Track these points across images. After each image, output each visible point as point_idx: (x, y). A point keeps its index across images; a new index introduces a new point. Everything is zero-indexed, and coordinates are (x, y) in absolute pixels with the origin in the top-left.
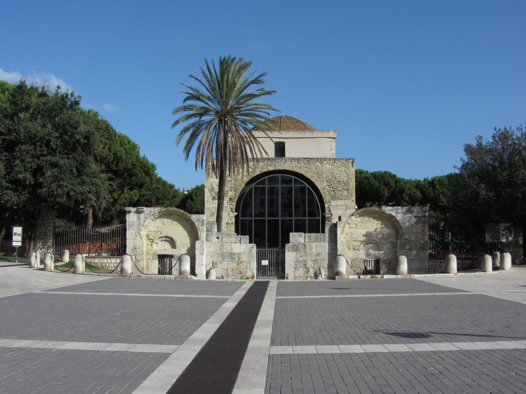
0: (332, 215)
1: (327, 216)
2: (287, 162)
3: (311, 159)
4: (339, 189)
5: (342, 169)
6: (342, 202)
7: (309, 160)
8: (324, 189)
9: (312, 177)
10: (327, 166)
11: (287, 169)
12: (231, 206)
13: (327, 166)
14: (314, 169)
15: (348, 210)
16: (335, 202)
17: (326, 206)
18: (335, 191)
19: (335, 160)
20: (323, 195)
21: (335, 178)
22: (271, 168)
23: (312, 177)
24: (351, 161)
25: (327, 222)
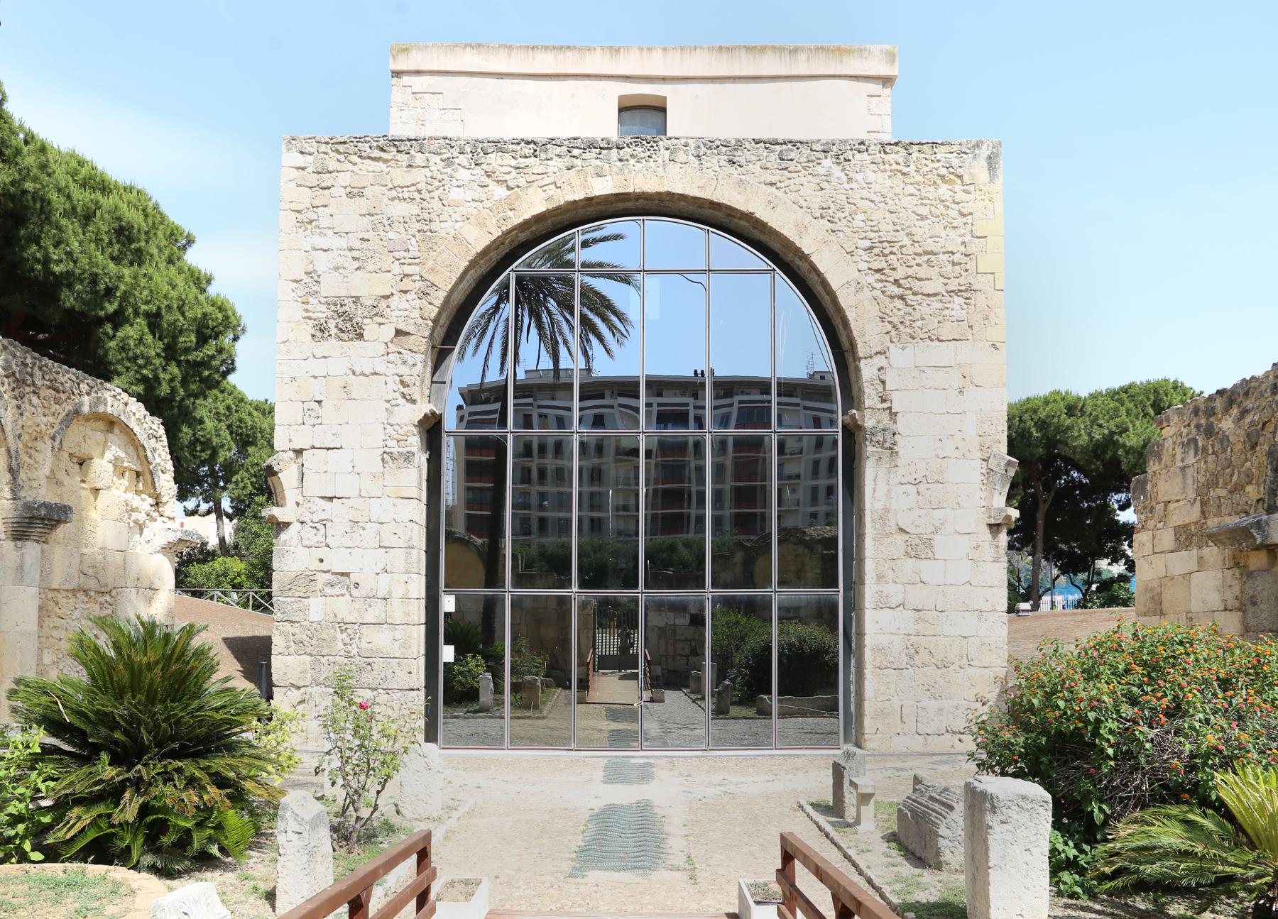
0: (893, 415)
1: (869, 423)
2: (681, 157)
3: (793, 143)
4: (929, 287)
5: (944, 190)
6: (941, 354)
7: (783, 149)
8: (859, 287)
9: (802, 228)
10: (871, 177)
11: (678, 189)
12: (404, 370)
13: (871, 177)
14: (809, 190)
15: (971, 391)
16: (910, 350)
17: (868, 371)
18: (910, 298)
19: (907, 146)
20: (851, 315)
21: (910, 234)
22: (602, 187)
23: (802, 228)
24: (984, 152)
25: (870, 449)
